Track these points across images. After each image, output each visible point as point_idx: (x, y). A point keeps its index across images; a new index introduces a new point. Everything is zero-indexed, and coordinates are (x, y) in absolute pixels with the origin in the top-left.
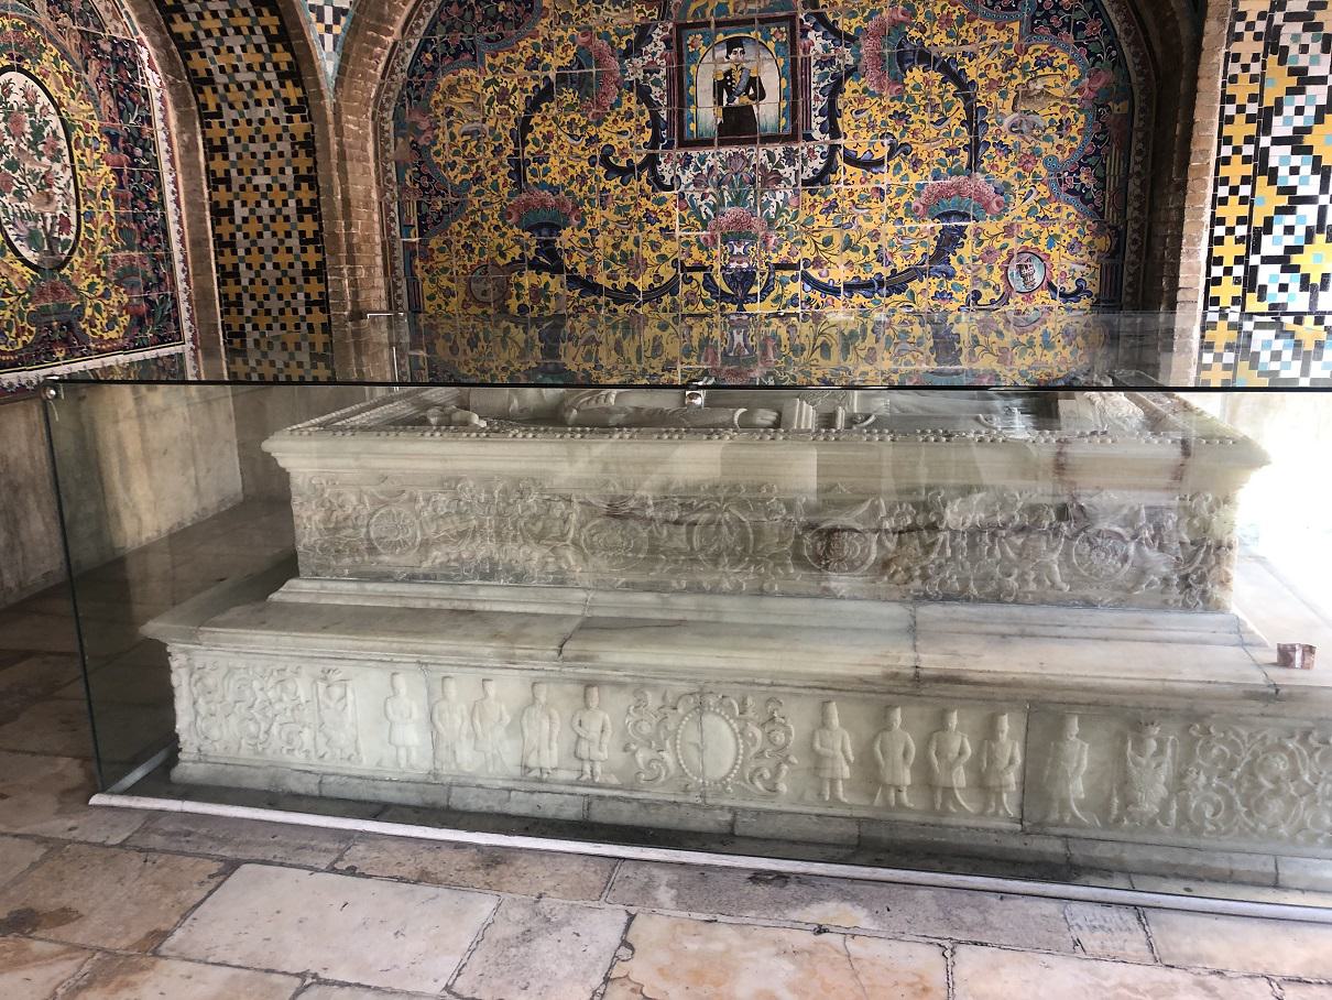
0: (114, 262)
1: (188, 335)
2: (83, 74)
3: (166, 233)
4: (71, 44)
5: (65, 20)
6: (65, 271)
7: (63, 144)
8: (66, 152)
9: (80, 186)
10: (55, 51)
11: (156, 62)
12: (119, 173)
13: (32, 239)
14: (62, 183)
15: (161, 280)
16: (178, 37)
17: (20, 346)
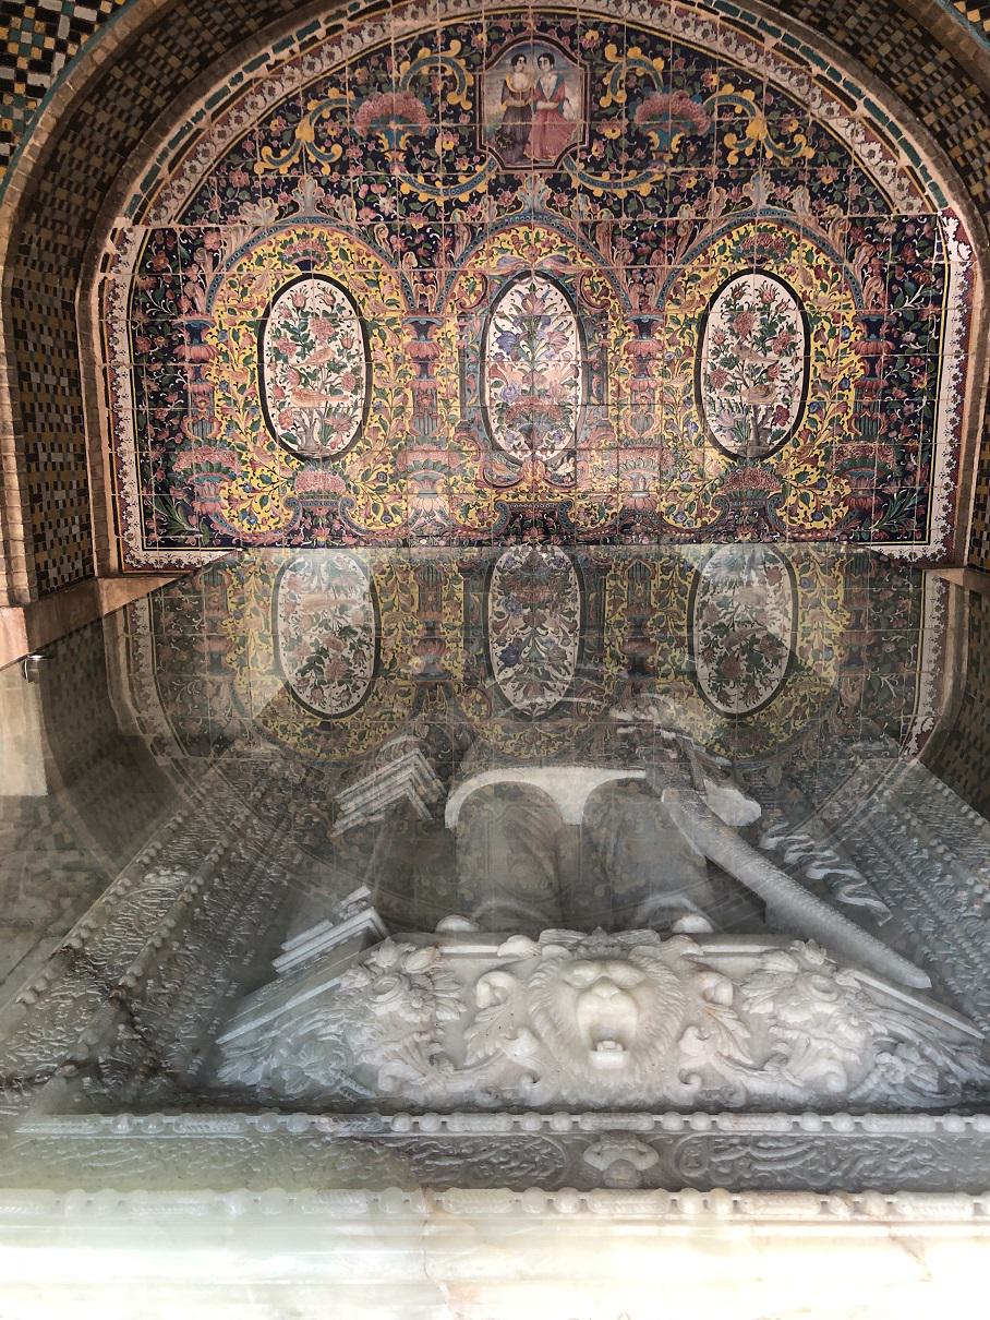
0: (840, 452)
1: (936, 535)
2: (846, 263)
3: (930, 422)
4: (833, 237)
5: (833, 211)
6: (771, 460)
7: (800, 337)
8: (802, 345)
9: (811, 376)
10: (810, 246)
11: (968, 232)
12: (873, 362)
13: (737, 430)
14: (787, 377)
15: (907, 474)
16: (976, 199)
17: (699, 525)
